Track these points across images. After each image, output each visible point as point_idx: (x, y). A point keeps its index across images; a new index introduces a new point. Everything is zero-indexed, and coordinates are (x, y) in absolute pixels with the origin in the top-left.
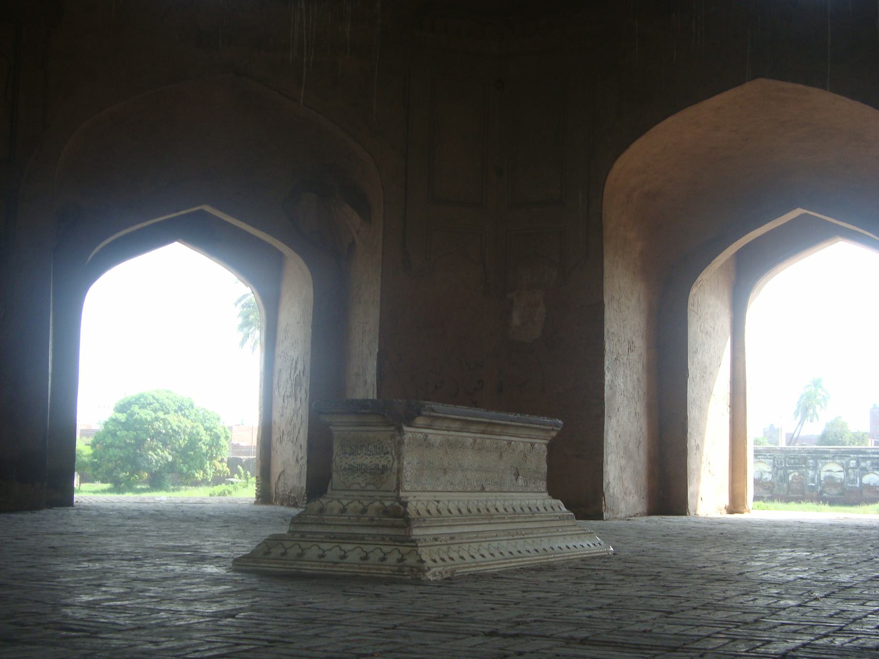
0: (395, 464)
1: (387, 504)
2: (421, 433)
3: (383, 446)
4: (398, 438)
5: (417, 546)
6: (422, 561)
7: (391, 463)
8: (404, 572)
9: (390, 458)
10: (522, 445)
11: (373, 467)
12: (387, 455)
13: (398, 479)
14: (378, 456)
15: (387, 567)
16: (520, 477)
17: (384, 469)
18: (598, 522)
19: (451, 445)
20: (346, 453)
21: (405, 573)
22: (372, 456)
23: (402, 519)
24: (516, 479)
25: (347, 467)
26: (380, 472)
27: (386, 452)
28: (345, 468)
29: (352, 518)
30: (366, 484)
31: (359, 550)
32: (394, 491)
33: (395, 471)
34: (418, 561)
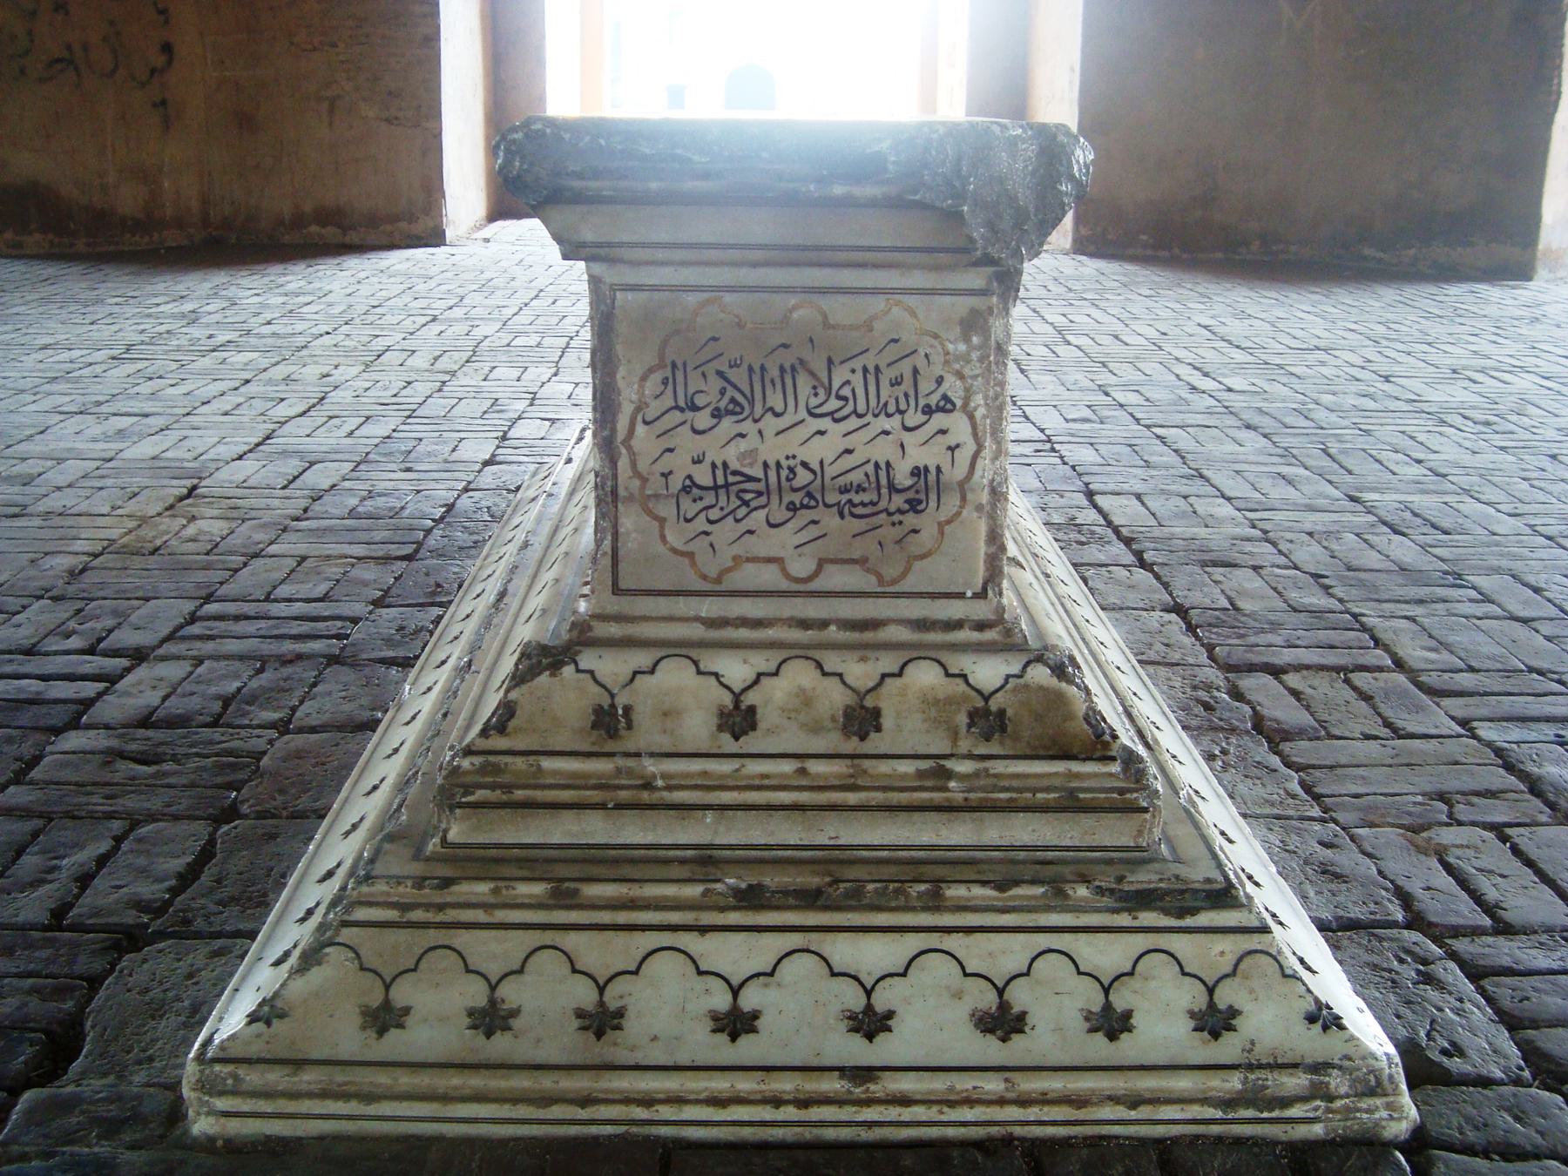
3: (916, 371)
7: (964, 456)
8: (1286, 1102)
11: (856, 477)
12: (939, 420)
14: (893, 424)
15: (1183, 1083)
20: (694, 408)
22: (854, 422)
25: (703, 476)
26: (898, 501)
27: (934, 400)
28: (690, 486)
29: (816, 767)
30: (821, 563)
31: (938, 970)
32: (981, 595)
33: (985, 497)
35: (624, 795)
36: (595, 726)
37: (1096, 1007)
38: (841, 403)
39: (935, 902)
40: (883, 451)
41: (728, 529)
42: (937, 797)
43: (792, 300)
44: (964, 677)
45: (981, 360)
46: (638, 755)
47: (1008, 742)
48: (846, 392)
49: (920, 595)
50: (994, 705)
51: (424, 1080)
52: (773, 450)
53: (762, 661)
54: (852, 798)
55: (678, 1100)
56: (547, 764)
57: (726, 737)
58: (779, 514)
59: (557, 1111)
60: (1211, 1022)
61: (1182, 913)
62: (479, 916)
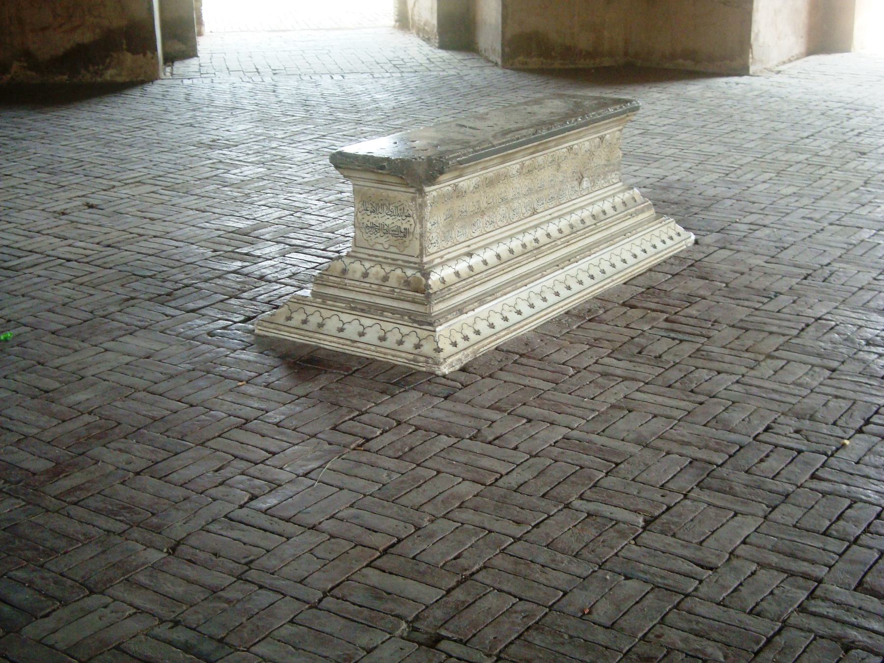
0: (418, 226)
1: (409, 272)
2: (449, 185)
4: (420, 201)
5: (435, 331)
6: (438, 350)
8: (419, 362)
9: (412, 222)
10: (588, 143)
11: (395, 229)
12: (408, 219)
13: (421, 245)
14: (400, 218)
15: (403, 355)
16: (585, 179)
17: (406, 233)
18: (744, 79)
19: (491, 183)
21: (420, 364)
23: (423, 295)
24: (580, 183)
28: (367, 226)
29: (373, 286)
32: (417, 257)
33: (418, 236)
34: (434, 350)
35: (341, 286)
39: (382, 315)
40: (399, 224)
41: (373, 237)
43: (382, 191)
52: (381, 221)
53: (372, 264)
54: (377, 293)
55: (325, 340)
56: (331, 278)
58: (382, 234)
62: (310, 304)
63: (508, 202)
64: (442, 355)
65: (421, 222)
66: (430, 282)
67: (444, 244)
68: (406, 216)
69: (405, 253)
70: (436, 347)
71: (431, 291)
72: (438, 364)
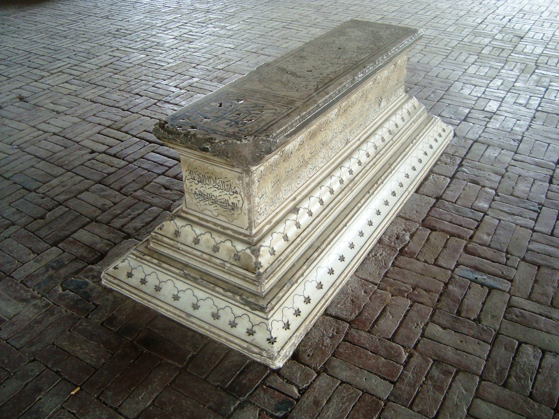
0: (246, 203)
4: (247, 180)
6: (272, 341)
9: (239, 198)
11: (222, 201)
12: (235, 195)
13: (250, 219)
14: (227, 193)
15: (237, 341)
17: (234, 207)
23: (254, 276)
27: (234, 191)
28: (195, 193)
30: (218, 214)
31: (209, 302)
32: (247, 230)
33: (246, 212)
36: (175, 234)
37: (232, 320)
38: (218, 186)
40: (227, 197)
41: (202, 203)
42: (222, 269)
43: (208, 165)
44: (235, 247)
45: (242, 186)
46: (178, 242)
47: (239, 263)
48: (219, 184)
49: (234, 225)
50: (239, 254)
51: (130, 289)
57: (194, 244)
59: (145, 301)
60: (251, 332)
61: (252, 310)
63: (327, 145)
64: (276, 346)
65: (249, 199)
66: (260, 260)
67: (272, 208)
68: (233, 192)
69: (233, 223)
70: (269, 337)
71: (261, 270)
72: (271, 358)
